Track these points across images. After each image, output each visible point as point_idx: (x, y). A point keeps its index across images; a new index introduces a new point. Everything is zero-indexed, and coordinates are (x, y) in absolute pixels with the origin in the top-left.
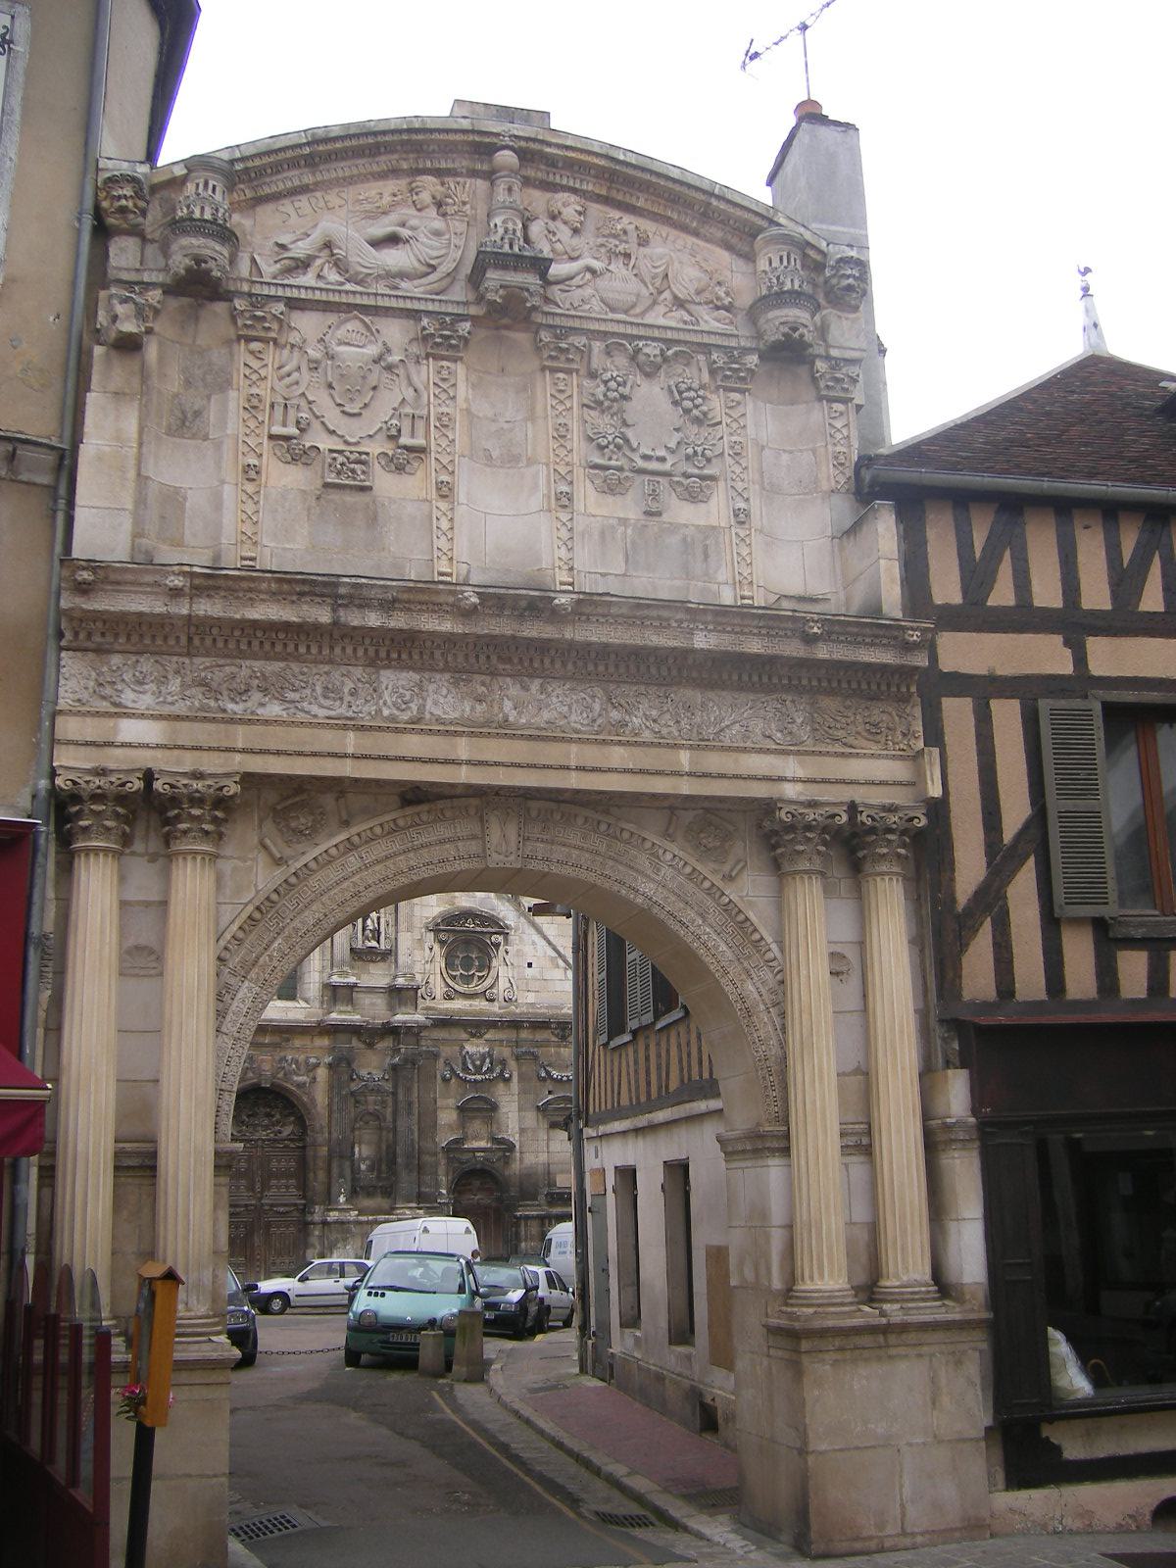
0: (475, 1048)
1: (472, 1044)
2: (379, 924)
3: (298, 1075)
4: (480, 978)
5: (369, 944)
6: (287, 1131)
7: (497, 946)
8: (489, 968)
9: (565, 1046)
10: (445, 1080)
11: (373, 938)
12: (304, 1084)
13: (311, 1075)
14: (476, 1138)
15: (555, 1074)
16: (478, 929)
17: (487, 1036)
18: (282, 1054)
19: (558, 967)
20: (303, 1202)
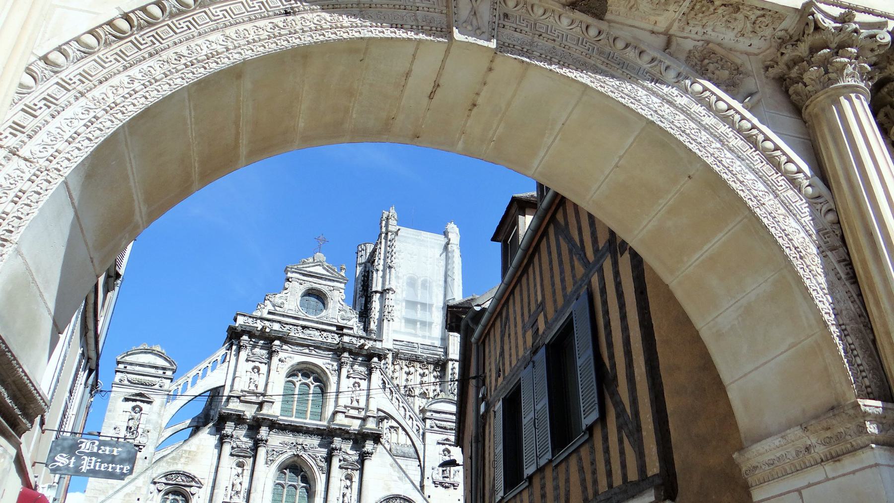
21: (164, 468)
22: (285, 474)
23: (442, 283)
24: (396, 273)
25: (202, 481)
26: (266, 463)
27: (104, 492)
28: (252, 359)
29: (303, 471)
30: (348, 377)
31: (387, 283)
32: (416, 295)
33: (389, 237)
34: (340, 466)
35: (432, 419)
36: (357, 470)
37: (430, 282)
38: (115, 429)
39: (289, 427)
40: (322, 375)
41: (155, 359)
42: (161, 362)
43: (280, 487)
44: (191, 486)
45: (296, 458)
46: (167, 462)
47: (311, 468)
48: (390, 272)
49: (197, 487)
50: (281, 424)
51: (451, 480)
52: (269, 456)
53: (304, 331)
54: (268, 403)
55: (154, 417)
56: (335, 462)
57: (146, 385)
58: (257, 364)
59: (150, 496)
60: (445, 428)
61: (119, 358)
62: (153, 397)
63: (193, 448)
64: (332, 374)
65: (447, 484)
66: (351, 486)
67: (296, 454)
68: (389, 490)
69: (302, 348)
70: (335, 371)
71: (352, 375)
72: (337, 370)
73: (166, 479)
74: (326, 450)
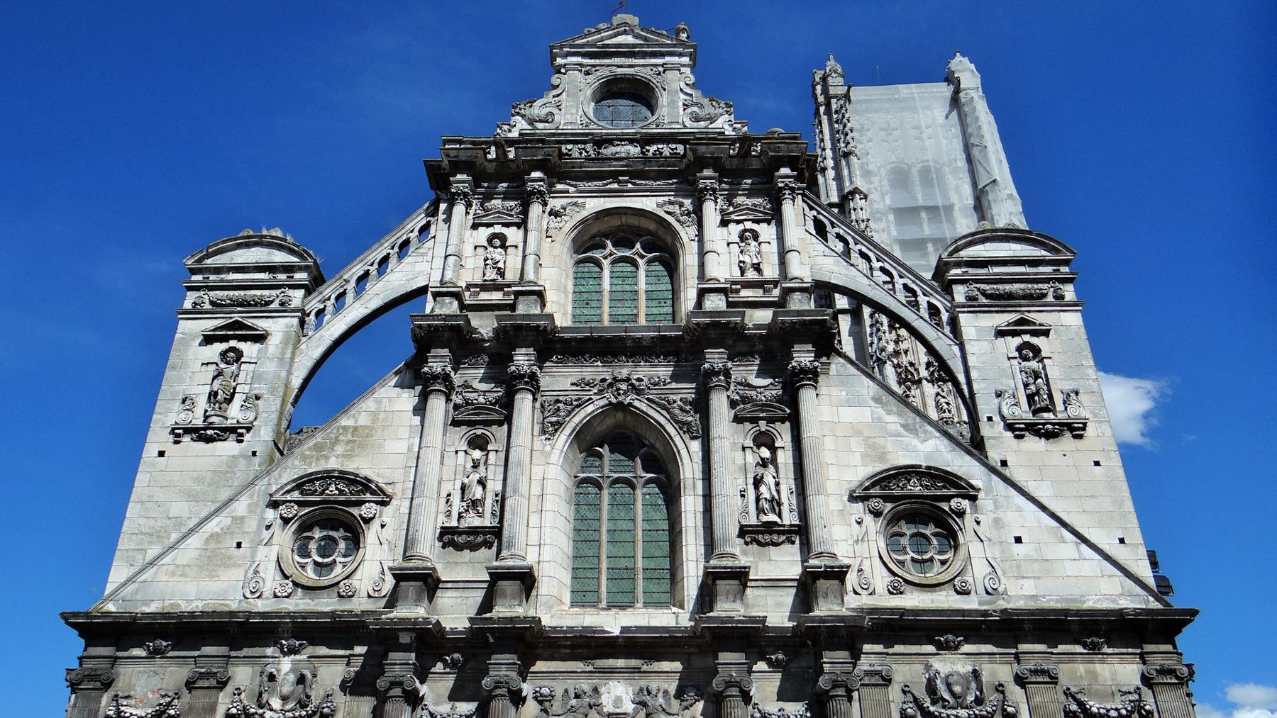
2: (778, 492)
5: (764, 518)
7: (961, 514)
8: (956, 547)
11: (773, 511)
16: (926, 493)
18: (643, 683)
21: (294, 468)
22: (600, 456)
23: (962, 163)
24: (862, 166)
25: (389, 490)
26: (544, 432)
28: (485, 220)
29: (644, 445)
30: (724, 223)
31: (847, 183)
32: (915, 198)
33: (834, 107)
34: (736, 416)
36: (783, 421)
37: (937, 170)
38: (184, 401)
40: (661, 232)
41: (269, 254)
42: (280, 257)
43: (592, 489)
44: (360, 503)
45: (620, 416)
46: (304, 458)
47: (659, 431)
48: (848, 164)
49: (377, 503)
50: (571, 339)
51: (1060, 416)
52: (547, 414)
53: (603, 151)
54: (526, 297)
55: (270, 367)
56: (720, 404)
57: (250, 305)
58: (498, 229)
59: (266, 535)
60: (1010, 296)
62: (262, 324)
63: (363, 420)
64: (682, 223)
65: (1050, 426)
66: (773, 461)
67: (614, 401)
68: (882, 458)
69: (600, 183)
70: (688, 214)
71: (733, 217)
72: (694, 212)
74: (694, 385)
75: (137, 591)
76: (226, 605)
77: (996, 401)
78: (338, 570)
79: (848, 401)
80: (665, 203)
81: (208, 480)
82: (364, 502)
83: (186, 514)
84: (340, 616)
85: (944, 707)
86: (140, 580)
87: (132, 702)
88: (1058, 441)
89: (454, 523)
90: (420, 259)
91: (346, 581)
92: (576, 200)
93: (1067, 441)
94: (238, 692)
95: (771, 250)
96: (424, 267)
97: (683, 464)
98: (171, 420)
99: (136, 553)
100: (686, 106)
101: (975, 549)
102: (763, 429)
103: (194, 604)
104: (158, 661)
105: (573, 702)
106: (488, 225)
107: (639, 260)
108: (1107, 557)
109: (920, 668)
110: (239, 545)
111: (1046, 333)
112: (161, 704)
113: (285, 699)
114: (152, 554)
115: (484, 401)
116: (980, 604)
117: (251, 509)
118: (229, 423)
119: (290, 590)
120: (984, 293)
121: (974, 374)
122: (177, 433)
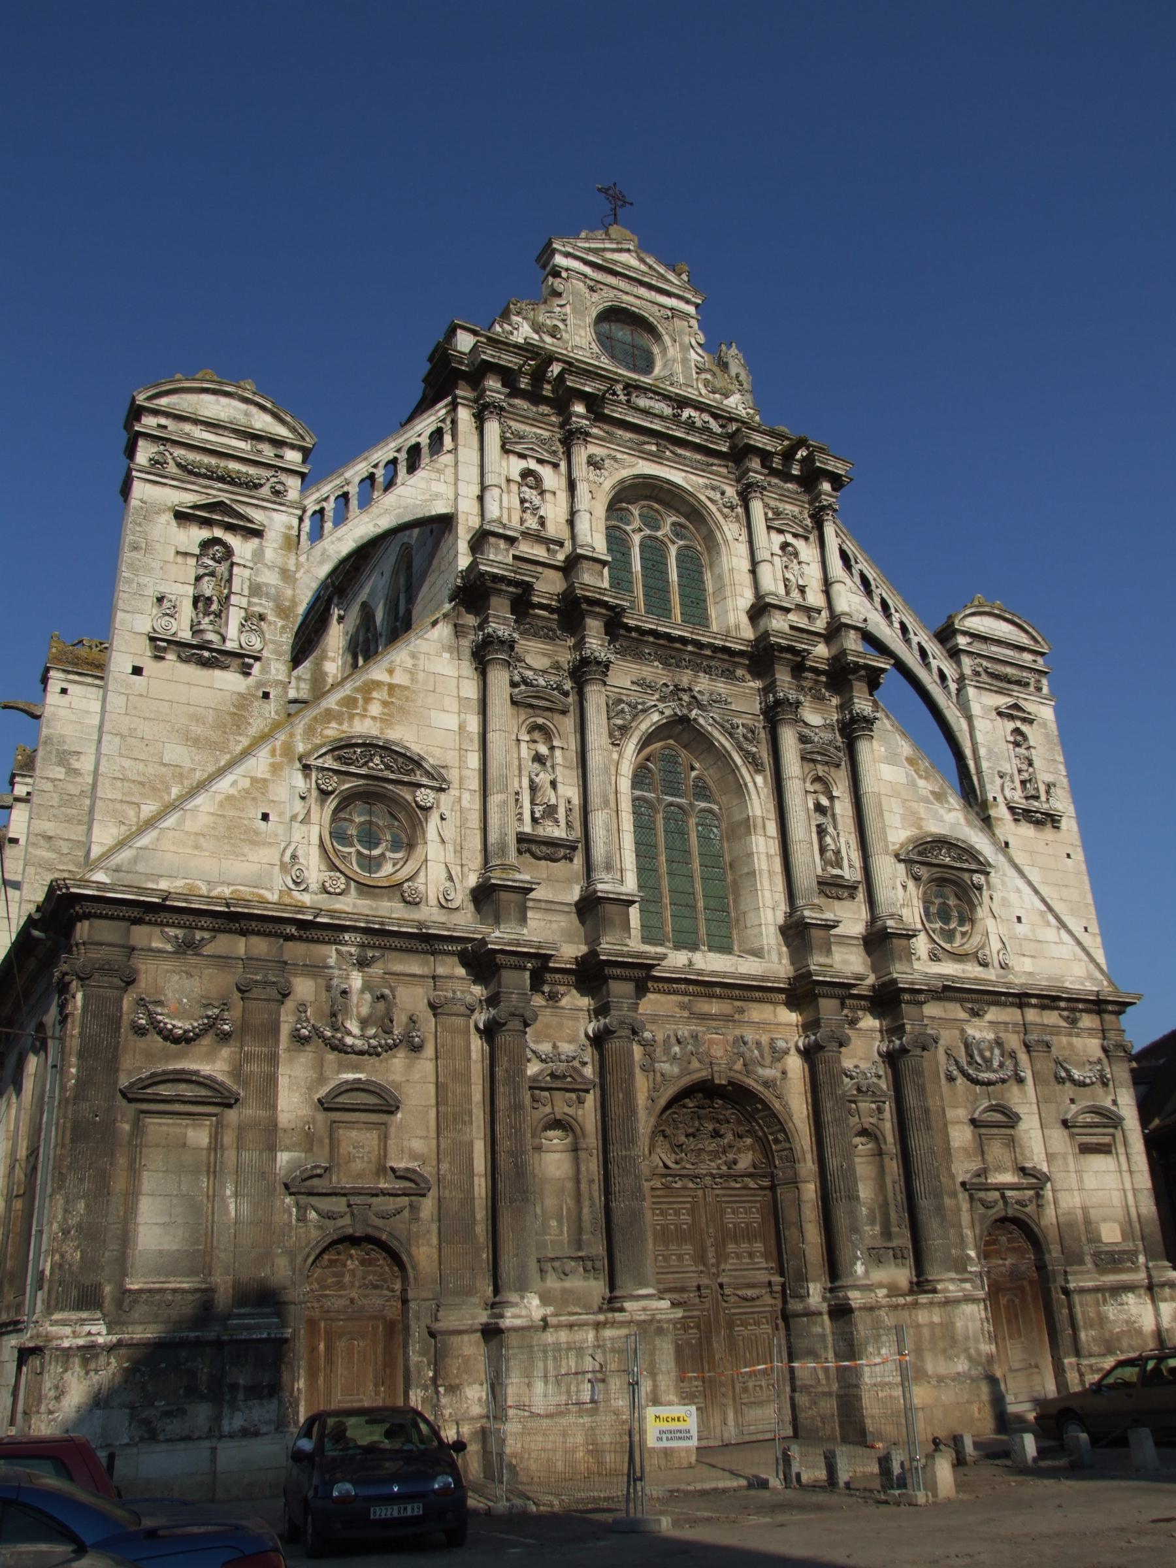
0: (979, 1031)
1: (975, 1027)
3: (763, 1066)
4: (964, 934)
6: (745, 1161)
7: (979, 888)
8: (972, 921)
9: (1078, 1035)
10: (951, 1079)
12: (774, 1080)
13: (779, 1065)
14: (1000, 1169)
15: (1076, 1074)
17: (989, 1017)
18: (738, 1032)
19: (1048, 924)
20: (780, 1279)
26: (611, 735)
27: (153, 789)
28: (518, 448)
29: (693, 768)
35: (973, 653)
39: (651, 639)
56: (789, 738)
57: (232, 482)
58: (532, 464)
61: (141, 399)
62: (257, 516)
63: (400, 678)
64: (725, 517)
65: (1038, 815)
67: (679, 713)
70: (732, 508)
73: (339, 759)
75: (135, 860)
76: (261, 896)
77: (998, 781)
78: (388, 868)
79: (887, 758)
80: (706, 487)
81: (210, 720)
82: (420, 786)
83: (187, 764)
84: (428, 927)
85: (977, 1069)
86: (138, 844)
87: (165, 1011)
88: (1042, 830)
89: (527, 828)
90: (434, 475)
91: (410, 883)
92: (613, 453)
93: (1048, 833)
94: (302, 1007)
95: (813, 574)
96: (442, 488)
97: (750, 799)
98: (144, 624)
99: (125, 807)
100: (700, 371)
101: (990, 924)
102: (821, 774)
103: (219, 889)
104: (193, 960)
105: (676, 1049)
106: (522, 456)
107: (670, 545)
108: (1079, 943)
109: (957, 1033)
110: (265, 817)
111: (1031, 722)
112: (208, 1017)
113: (364, 1023)
114: (149, 809)
115: (544, 684)
116: (997, 976)
117: (275, 768)
118: (230, 646)
119: (343, 886)
120: (986, 670)
121: (982, 752)
122: (160, 645)
